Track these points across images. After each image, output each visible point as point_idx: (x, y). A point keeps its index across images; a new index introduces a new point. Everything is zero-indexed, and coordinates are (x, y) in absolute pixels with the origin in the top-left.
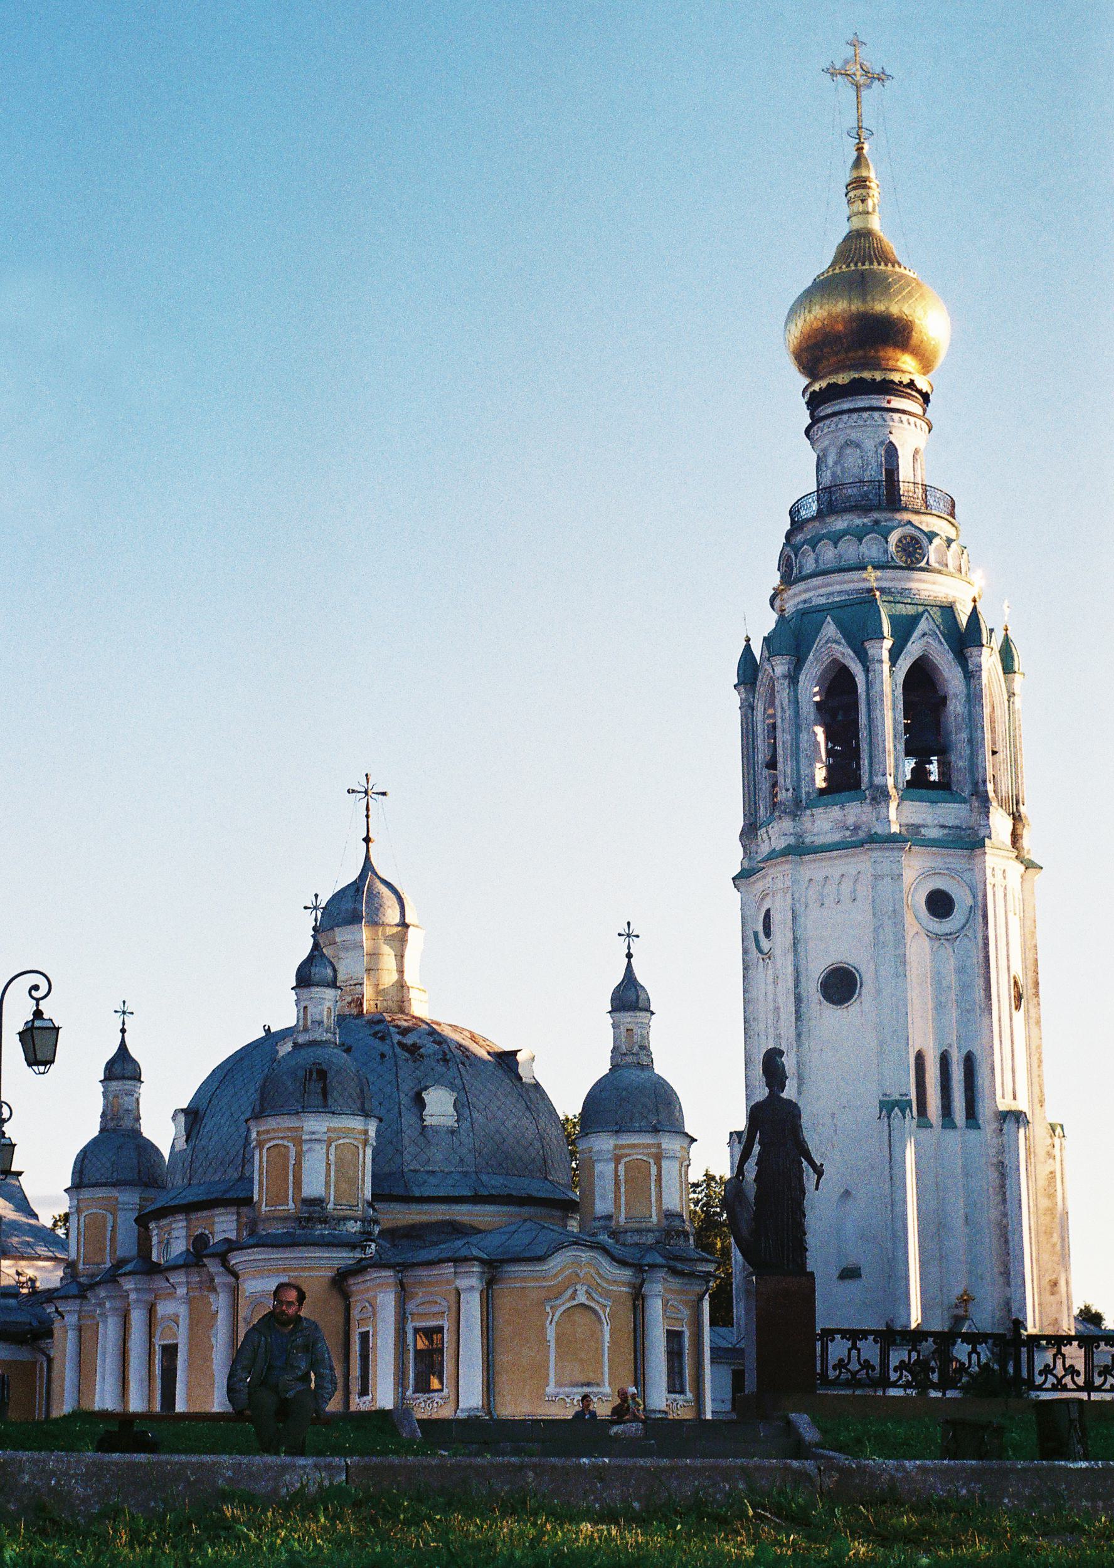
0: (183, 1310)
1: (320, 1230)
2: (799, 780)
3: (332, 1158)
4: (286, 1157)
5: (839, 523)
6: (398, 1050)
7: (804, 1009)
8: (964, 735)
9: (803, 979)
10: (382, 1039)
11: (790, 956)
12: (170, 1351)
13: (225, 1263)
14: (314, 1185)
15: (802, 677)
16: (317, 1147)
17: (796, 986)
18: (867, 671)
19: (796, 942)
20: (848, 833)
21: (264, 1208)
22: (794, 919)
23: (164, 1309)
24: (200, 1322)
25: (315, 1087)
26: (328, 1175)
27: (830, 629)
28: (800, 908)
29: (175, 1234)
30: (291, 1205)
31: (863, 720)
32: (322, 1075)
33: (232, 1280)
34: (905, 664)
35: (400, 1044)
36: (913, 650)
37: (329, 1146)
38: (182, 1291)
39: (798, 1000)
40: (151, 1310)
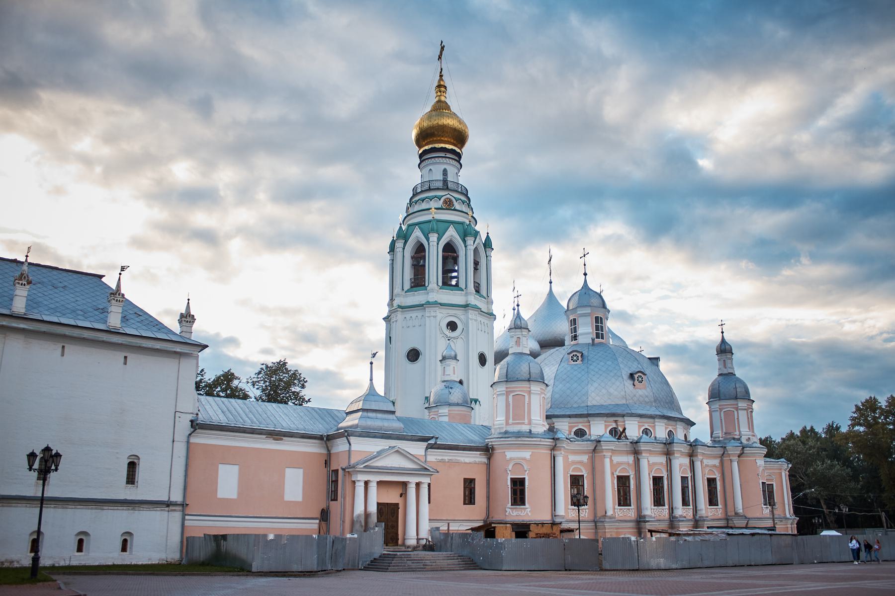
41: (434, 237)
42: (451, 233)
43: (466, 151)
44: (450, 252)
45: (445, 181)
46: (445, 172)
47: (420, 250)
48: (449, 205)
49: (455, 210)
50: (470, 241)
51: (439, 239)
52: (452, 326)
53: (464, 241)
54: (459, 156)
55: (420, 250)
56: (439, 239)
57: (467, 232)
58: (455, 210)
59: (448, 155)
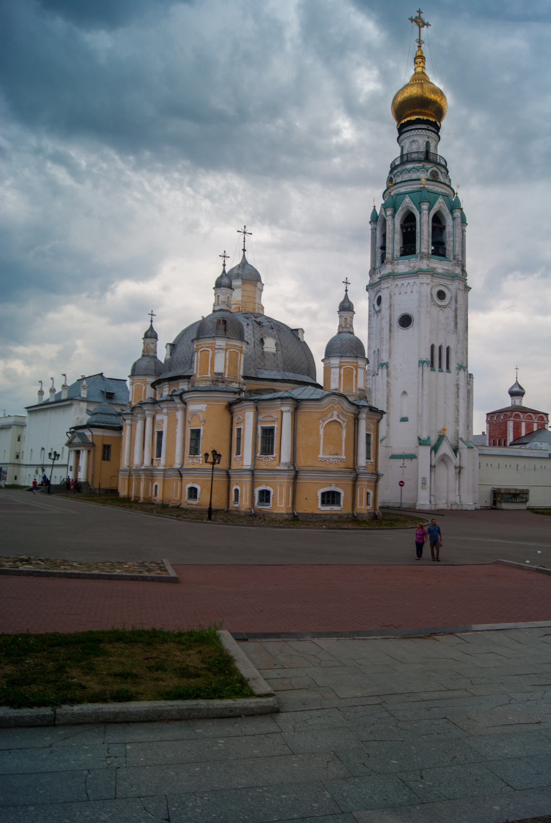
0: (165, 418)
1: (221, 386)
2: (393, 250)
3: (227, 356)
4: (208, 355)
5: (409, 166)
6: (254, 323)
7: (392, 329)
8: (452, 239)
9: (392, 318)
10: (248, 318)
11: (388, 310)
12: (160, 434)
13: (181, 399)
14: (219, 367)
15: (396, 216)
16: (221, 351)
17: (390, 321)
18: (420, 213)
19: (390, 305)
20: (411, 269)
21: (198, 376)
22: (391, 297)
23: (159, 417)
24: (172, 423)
25: (222, 326)
26: (225, 363)
27: (407, 200)
28: (392, 294)
29: (164, 389)
30: (209, 375)
31: (418, 230)
32: (225, 322)
33: (183, 405)
34: (432, 213)
35: (254, 321)
36: (436, 207)
37: (226, 351)
38: (165, 411)
39: (390, 325)
40: (154, 418)
41: (425, 206)
42: (440, 204)
43: (445, 124)
44: (438, 222)
45: (427, 152)
46: (428, 144)
47: (409, 220)
48: (434, 178)
49: (440, 182)
50: (457, 214)
51: (430, 210)
52: (441, 295)
53: (452, 212)
54: (438, 128)
55: (409, 220)
56: (430, 210)
57: (455, 206)
58: (440, 182)
59: (430, 128)
